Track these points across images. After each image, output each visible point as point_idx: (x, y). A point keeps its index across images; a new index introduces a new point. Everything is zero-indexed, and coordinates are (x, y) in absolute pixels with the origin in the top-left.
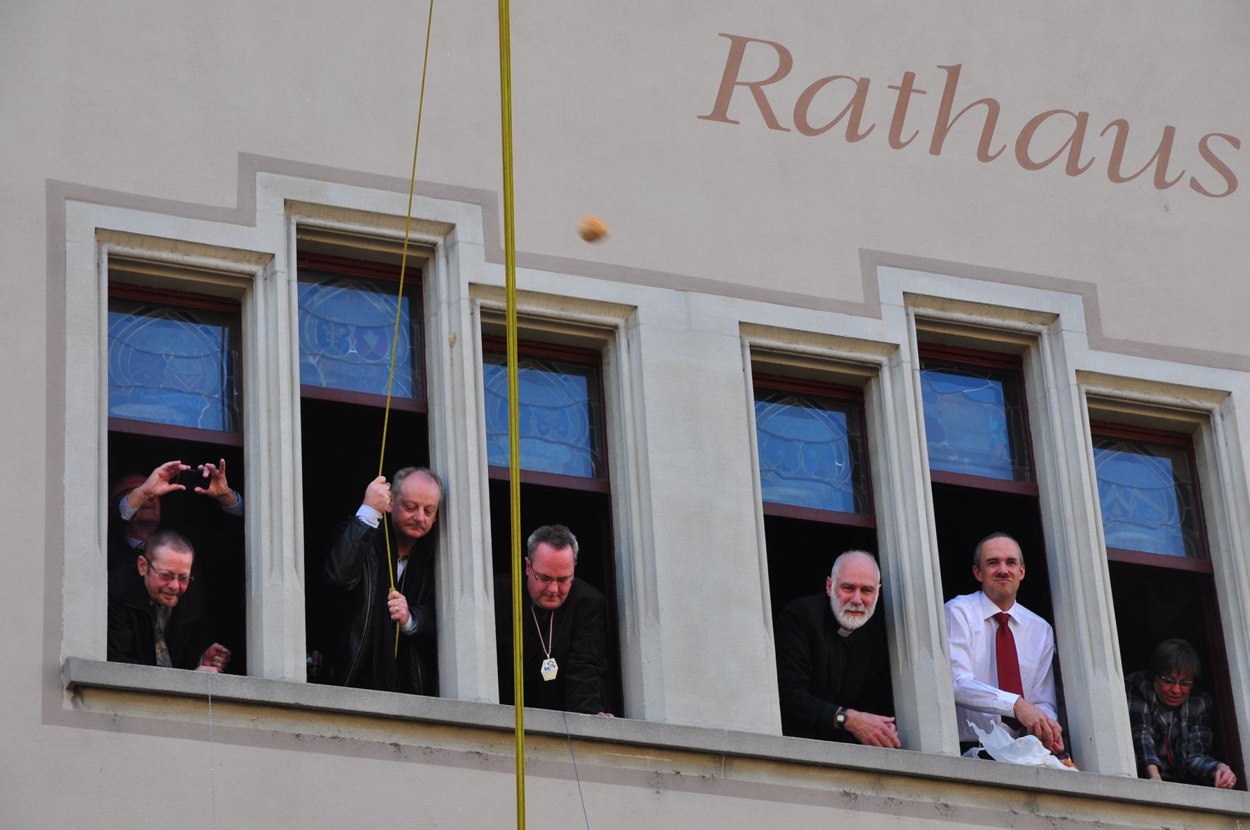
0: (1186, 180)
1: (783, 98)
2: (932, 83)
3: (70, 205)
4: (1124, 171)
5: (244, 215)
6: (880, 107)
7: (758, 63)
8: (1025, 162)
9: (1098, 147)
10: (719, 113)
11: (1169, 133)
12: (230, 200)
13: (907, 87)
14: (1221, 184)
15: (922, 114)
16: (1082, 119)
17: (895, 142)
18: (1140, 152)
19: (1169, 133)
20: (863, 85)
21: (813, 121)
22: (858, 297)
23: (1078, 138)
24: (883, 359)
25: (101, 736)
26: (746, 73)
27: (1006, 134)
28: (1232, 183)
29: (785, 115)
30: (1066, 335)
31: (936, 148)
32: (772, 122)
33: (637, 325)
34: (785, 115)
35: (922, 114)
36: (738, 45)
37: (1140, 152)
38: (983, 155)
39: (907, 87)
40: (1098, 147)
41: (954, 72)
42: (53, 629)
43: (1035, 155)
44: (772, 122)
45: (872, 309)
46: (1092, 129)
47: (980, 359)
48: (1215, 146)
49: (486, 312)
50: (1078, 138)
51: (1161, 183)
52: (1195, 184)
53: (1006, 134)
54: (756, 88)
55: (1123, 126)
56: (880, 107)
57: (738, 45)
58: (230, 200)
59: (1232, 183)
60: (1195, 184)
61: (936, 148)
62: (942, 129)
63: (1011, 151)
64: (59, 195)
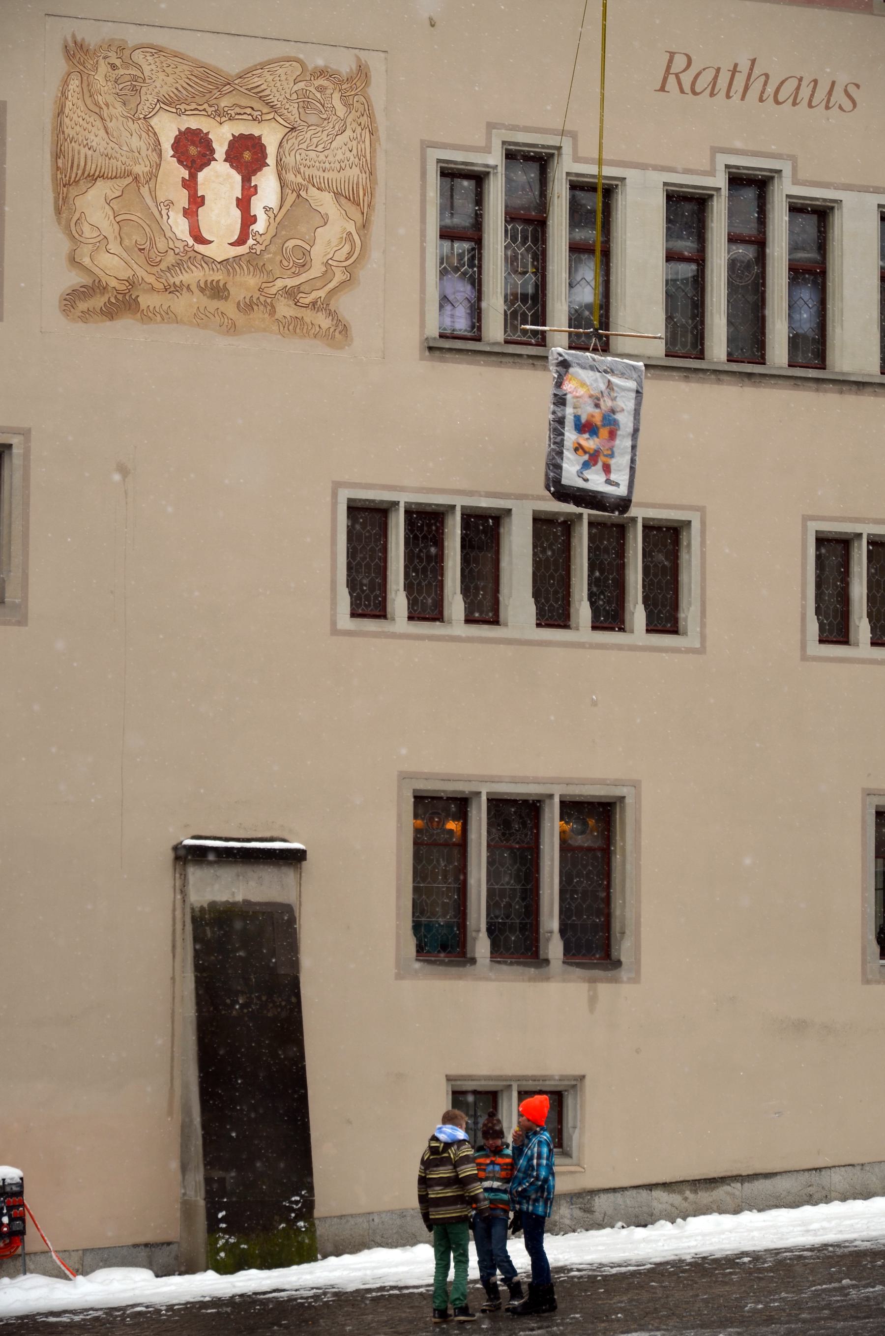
0: (837, 105)
1: (687, 79)
2: (744, 67)
3: (429, 150)
4: (813, 104)
5: (487, 150)
7: (680, 62)
8: (777, 102)
9: (805, 92)
10: (662, 89)
11: (833, 83)
12: (483, 144)
13: (734, 71)
14: (851, 105)
15: (740, 81)
17: (728, 96)
18: (821, 94)
20: (718, 70)
21: (698, 90)
22: (708, 168)
23: (798, 88)
24: (714, 193)
25: (437, 364)
26: (673, 70)
27: (770, 90)
28: (855, 104)
29: (687, 88)
30: (784, 179)
31: (743, 98)
32: (682, 91)
33: (625, 185)
34: (687, 88)
35: (740, 81)
36: (672, 55)
37: (821, 94)
38: (761, 100)
39: (734, 71)
40: (805, 92)
41: (753, 61)
42: (423, 325)
43: (781, 98)
44: (682, 91)
45: (712, 173)
46: (804, 83)
48: (852, 89)
49: (570, 181)
50: (798, 88)
51: (827, 107)
52: (840, 108)
53: (770, 90)
54: (677, 75)
55: (816, 82)
57: (672, 55)
58: (483, 144)
59: (855, 104)
60: (840, 108)
61: (743, 98)
62: (746, 88)
63: (771, 98)
64: (426, 145)
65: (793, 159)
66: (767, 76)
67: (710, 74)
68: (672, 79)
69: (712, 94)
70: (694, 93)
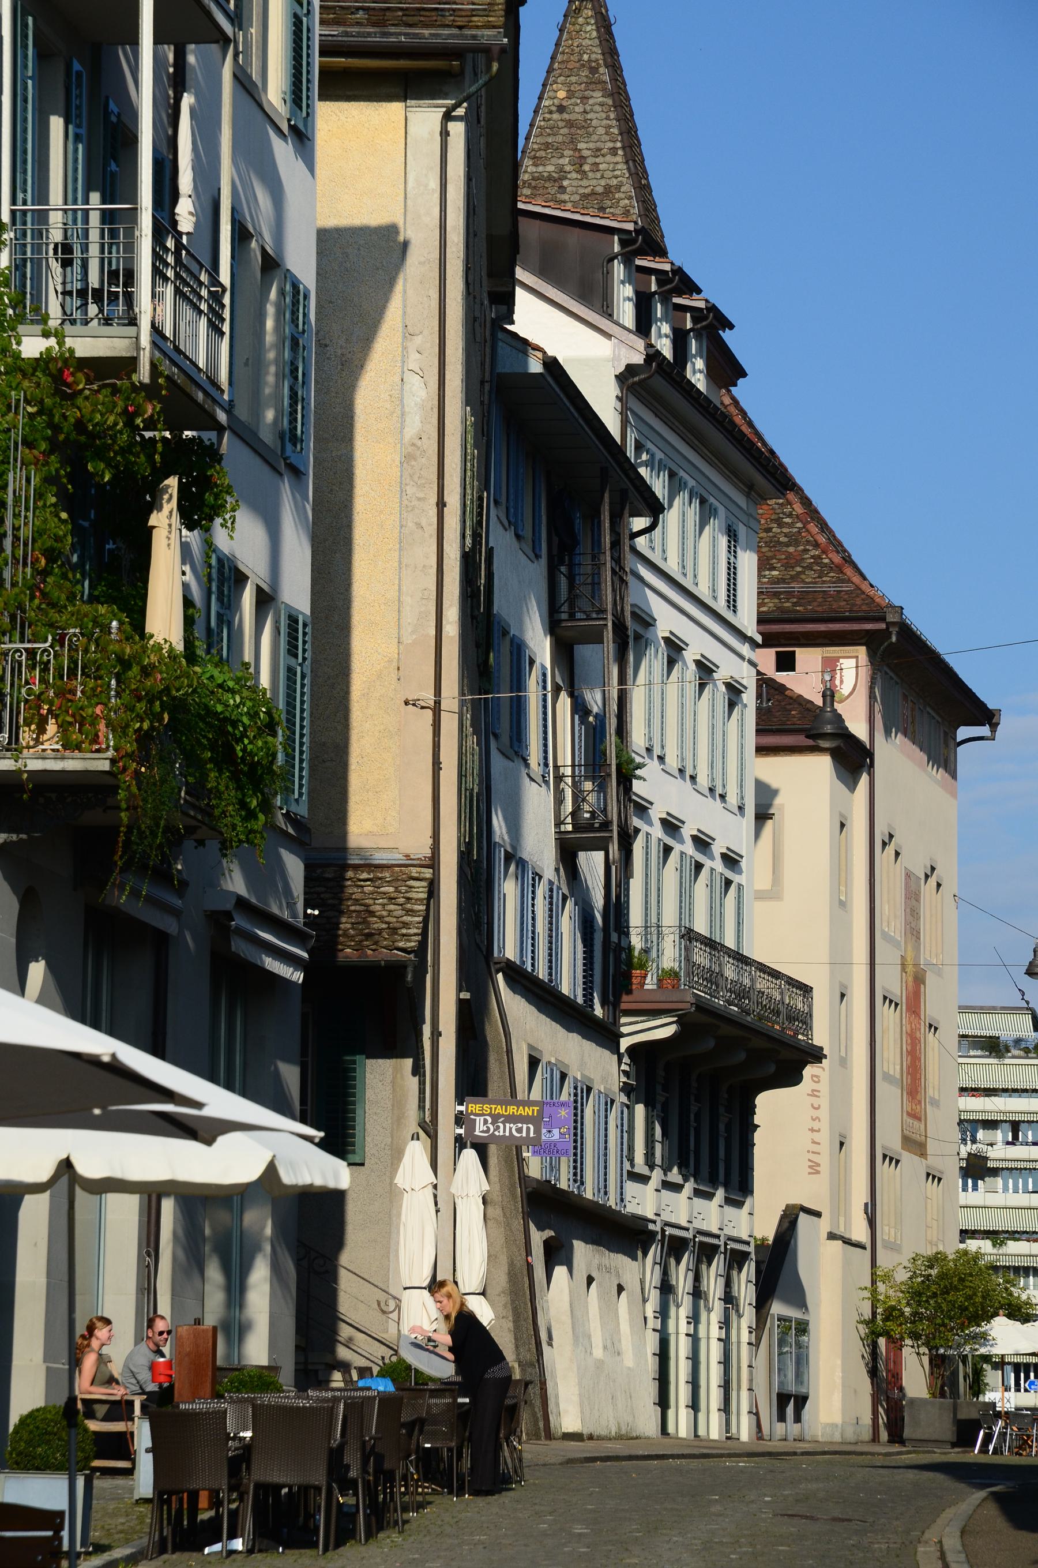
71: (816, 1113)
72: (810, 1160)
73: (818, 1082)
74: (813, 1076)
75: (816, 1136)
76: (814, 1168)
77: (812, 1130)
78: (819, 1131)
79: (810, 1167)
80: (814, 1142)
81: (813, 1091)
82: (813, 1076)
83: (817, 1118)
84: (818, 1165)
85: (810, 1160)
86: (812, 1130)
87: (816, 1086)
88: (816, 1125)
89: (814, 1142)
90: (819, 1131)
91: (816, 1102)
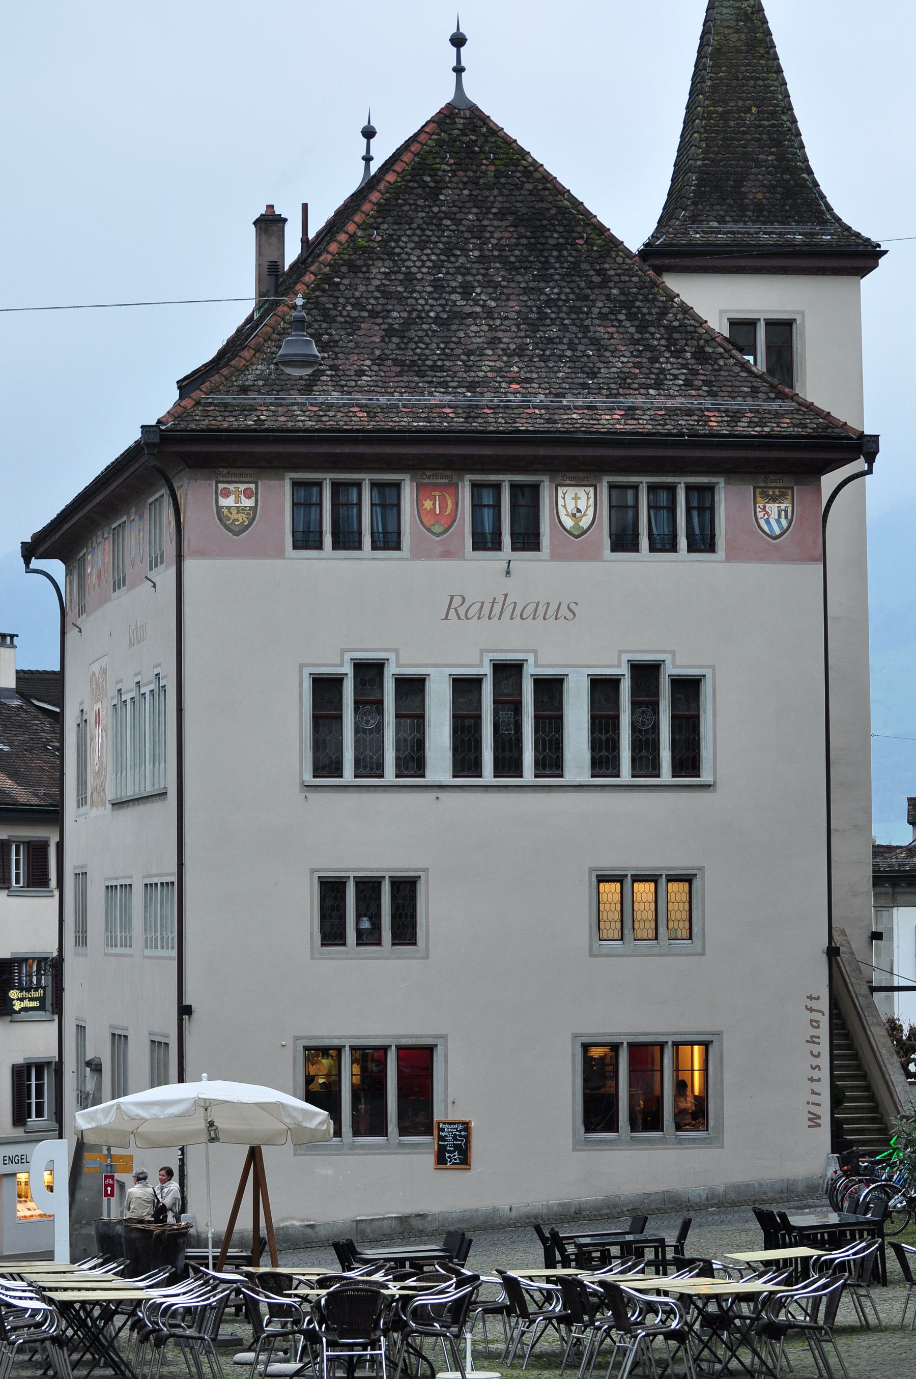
2: (500, 600)
6: (486, 610)
7: (457, 601)
9: (541, 611)
11: (560, 603)
15: (497, 609)
16: (538, 604)
17: (490, 618)
19: (560, 603)
20: (483, 603)
28: (575, 615)
29: (462, 616)
32: (459, 618)
34: (462, 616)
35: (497, 609)
36: (452, 597)
38: (512, 618)
40: (541, 611)
41: (506, 595)
44: (459, 618)
47: (508, 672)
51: (556, 619)
52: (565, 618)
54: (456, 609)
55: (548, 604)
56: (486, 610)
57: (452, 597)
60: (565, 618)
65: (535, 652)
66: (515, 603)
67: (479, 605)
68: (452, 611)
69: (479, 618)
70: (468, 619)
71: (815, 1062)
72: (809, 1112)
73: (818, 1027)
74: (812, 1021)
75: (815, 1086)
76: (814, 1121)
77: (812, 1080)
78: (819, 1080)
79: (810, 1119)
80: (814, 1093)
81: (812, 1037)
82: (812, 1021)
83: (818, 1066)
84: (819, 1117)
85: (809, 1112)
86: (812, 1080)
87: (815, 1032)
88: (816, 1074)
89: (814, 1093)
90: (819, 1080)
91: (815, 1049)
